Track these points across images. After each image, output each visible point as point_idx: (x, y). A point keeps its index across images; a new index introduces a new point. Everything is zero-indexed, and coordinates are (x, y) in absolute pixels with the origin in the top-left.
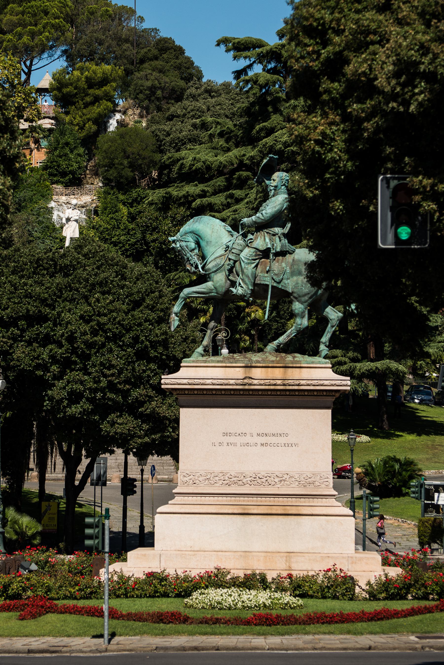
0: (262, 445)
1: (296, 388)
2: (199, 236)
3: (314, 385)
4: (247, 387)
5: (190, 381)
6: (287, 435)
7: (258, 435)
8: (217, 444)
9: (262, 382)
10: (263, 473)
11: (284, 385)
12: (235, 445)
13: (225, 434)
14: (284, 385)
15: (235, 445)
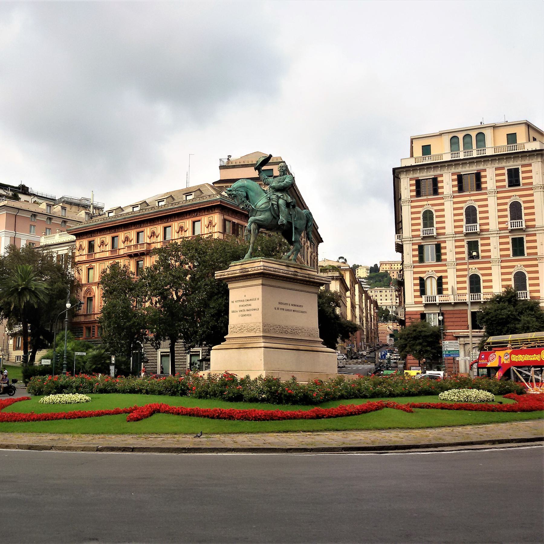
1: (313, 280)
2: (250, 189)
3: (319, 280)
4: (296, 277)
5: (274, 269)
7: (292, 305)
8: (276, 309)
9: (302, 275)
10: (294, 327)
11: (309, 278)
12: (284, 309)
13: (280, 303)
14: (309, 278)
15: (284, 309)
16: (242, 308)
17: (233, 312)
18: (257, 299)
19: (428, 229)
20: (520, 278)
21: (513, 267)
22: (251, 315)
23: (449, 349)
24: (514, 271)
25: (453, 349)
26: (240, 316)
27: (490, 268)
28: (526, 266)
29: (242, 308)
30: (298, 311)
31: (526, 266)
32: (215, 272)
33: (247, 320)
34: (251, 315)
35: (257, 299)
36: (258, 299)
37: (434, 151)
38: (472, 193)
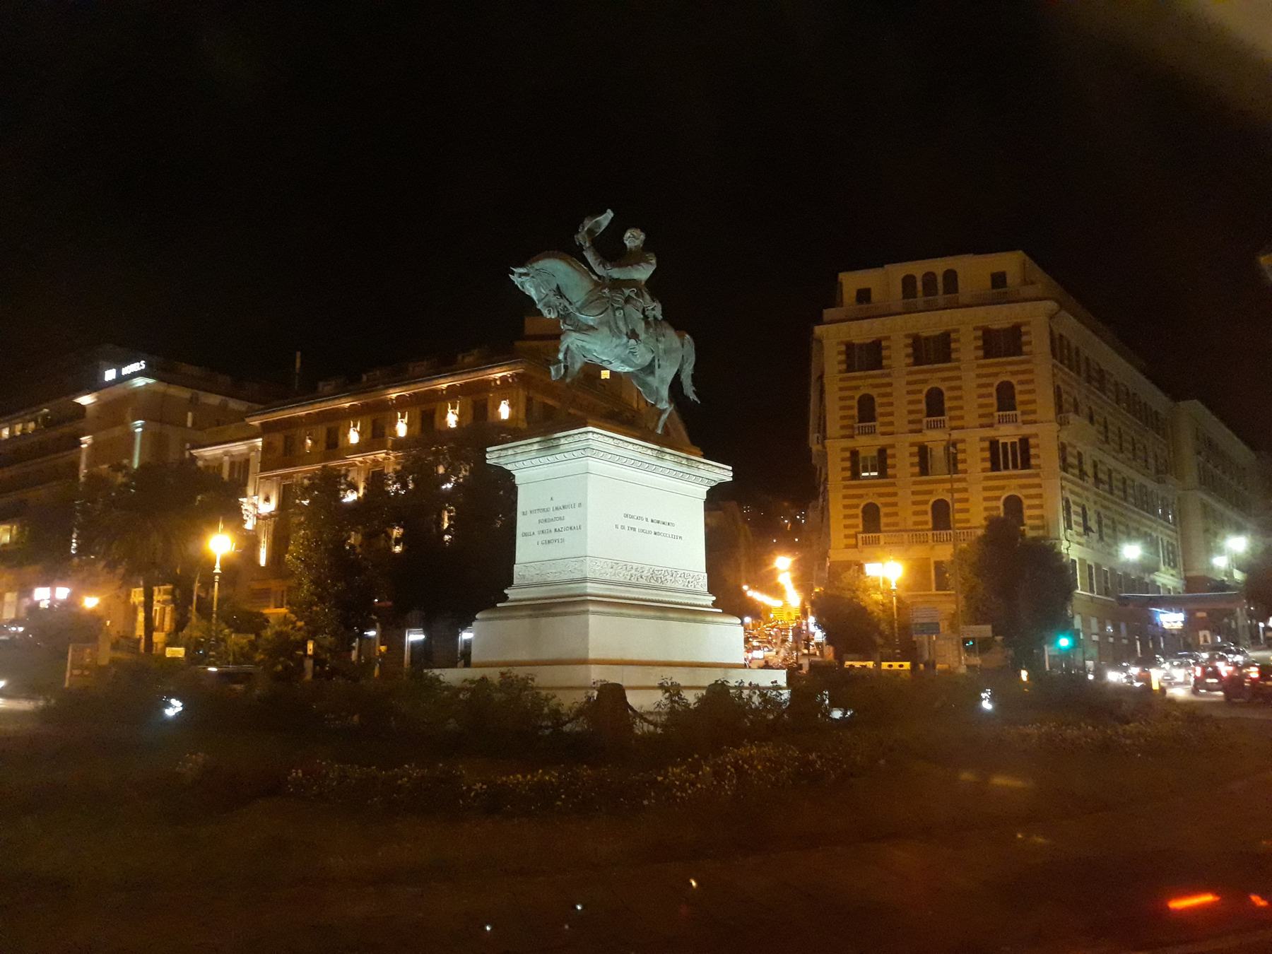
0: (655, 534)
6: (673, 525)
7: (652, 521)
13: (626, 516)
15: (634, 529)
16: (544, 526)
17: (525, 535)
18: (577, 505)
19: (867, 424)
20: (1014, 505)
23: (920, 621)
26: (540, 543)
29: (544, 526)
30: (665, 535)
32: (488, 449)
34: (563, 540)
35: (577, 505)
37: (875, 296)
38: (936, 366)
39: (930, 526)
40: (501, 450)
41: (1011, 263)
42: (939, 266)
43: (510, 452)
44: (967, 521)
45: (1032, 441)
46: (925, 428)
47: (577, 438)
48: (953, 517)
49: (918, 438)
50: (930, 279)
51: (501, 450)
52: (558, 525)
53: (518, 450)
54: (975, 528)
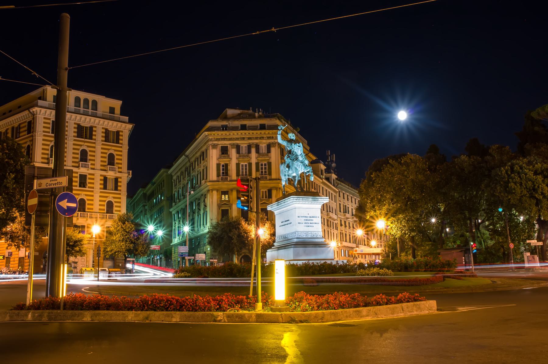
16: (306, 222)
21: (107, 197)
22: (313, 226)
24: (108, 200)
25: (184, 252)
27: (92, 196)
28: (114, 198)
29: (306, 222)
31: (114, 198)
33: (310, 229)
34: (313, 226)
36: (318, 217)
38: (86, 140)
39: (105, 211)
40: (298, 198)
41: (117, 104)
42: (91, 97)
43: (301, 199)
44: (92, 209)
45: (119, 180)
46: (109, 169)
47: (324, 199)
48: (77, 205)
49: (104, 173)
50: (86, 101)
51: (298, 198)
52: (311, 222)
53: (304, 199)
54: (95, 212)
